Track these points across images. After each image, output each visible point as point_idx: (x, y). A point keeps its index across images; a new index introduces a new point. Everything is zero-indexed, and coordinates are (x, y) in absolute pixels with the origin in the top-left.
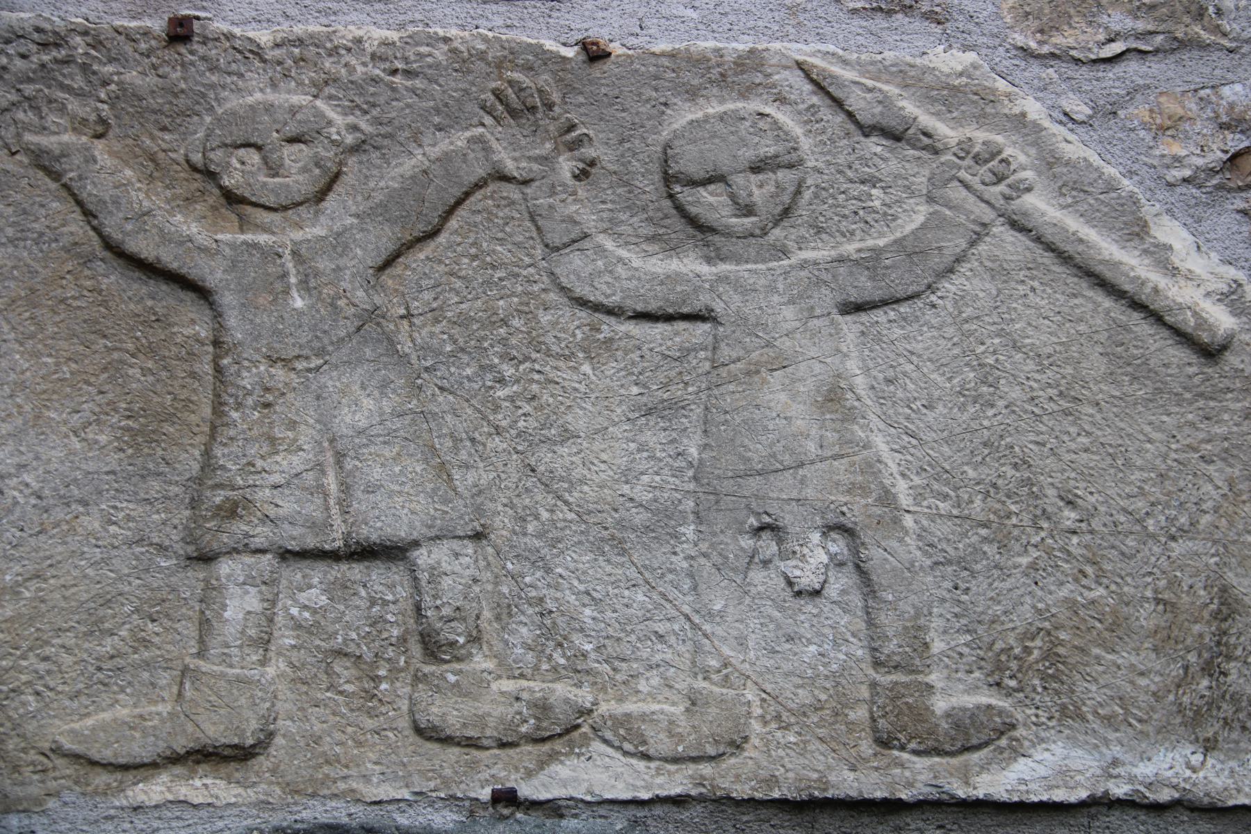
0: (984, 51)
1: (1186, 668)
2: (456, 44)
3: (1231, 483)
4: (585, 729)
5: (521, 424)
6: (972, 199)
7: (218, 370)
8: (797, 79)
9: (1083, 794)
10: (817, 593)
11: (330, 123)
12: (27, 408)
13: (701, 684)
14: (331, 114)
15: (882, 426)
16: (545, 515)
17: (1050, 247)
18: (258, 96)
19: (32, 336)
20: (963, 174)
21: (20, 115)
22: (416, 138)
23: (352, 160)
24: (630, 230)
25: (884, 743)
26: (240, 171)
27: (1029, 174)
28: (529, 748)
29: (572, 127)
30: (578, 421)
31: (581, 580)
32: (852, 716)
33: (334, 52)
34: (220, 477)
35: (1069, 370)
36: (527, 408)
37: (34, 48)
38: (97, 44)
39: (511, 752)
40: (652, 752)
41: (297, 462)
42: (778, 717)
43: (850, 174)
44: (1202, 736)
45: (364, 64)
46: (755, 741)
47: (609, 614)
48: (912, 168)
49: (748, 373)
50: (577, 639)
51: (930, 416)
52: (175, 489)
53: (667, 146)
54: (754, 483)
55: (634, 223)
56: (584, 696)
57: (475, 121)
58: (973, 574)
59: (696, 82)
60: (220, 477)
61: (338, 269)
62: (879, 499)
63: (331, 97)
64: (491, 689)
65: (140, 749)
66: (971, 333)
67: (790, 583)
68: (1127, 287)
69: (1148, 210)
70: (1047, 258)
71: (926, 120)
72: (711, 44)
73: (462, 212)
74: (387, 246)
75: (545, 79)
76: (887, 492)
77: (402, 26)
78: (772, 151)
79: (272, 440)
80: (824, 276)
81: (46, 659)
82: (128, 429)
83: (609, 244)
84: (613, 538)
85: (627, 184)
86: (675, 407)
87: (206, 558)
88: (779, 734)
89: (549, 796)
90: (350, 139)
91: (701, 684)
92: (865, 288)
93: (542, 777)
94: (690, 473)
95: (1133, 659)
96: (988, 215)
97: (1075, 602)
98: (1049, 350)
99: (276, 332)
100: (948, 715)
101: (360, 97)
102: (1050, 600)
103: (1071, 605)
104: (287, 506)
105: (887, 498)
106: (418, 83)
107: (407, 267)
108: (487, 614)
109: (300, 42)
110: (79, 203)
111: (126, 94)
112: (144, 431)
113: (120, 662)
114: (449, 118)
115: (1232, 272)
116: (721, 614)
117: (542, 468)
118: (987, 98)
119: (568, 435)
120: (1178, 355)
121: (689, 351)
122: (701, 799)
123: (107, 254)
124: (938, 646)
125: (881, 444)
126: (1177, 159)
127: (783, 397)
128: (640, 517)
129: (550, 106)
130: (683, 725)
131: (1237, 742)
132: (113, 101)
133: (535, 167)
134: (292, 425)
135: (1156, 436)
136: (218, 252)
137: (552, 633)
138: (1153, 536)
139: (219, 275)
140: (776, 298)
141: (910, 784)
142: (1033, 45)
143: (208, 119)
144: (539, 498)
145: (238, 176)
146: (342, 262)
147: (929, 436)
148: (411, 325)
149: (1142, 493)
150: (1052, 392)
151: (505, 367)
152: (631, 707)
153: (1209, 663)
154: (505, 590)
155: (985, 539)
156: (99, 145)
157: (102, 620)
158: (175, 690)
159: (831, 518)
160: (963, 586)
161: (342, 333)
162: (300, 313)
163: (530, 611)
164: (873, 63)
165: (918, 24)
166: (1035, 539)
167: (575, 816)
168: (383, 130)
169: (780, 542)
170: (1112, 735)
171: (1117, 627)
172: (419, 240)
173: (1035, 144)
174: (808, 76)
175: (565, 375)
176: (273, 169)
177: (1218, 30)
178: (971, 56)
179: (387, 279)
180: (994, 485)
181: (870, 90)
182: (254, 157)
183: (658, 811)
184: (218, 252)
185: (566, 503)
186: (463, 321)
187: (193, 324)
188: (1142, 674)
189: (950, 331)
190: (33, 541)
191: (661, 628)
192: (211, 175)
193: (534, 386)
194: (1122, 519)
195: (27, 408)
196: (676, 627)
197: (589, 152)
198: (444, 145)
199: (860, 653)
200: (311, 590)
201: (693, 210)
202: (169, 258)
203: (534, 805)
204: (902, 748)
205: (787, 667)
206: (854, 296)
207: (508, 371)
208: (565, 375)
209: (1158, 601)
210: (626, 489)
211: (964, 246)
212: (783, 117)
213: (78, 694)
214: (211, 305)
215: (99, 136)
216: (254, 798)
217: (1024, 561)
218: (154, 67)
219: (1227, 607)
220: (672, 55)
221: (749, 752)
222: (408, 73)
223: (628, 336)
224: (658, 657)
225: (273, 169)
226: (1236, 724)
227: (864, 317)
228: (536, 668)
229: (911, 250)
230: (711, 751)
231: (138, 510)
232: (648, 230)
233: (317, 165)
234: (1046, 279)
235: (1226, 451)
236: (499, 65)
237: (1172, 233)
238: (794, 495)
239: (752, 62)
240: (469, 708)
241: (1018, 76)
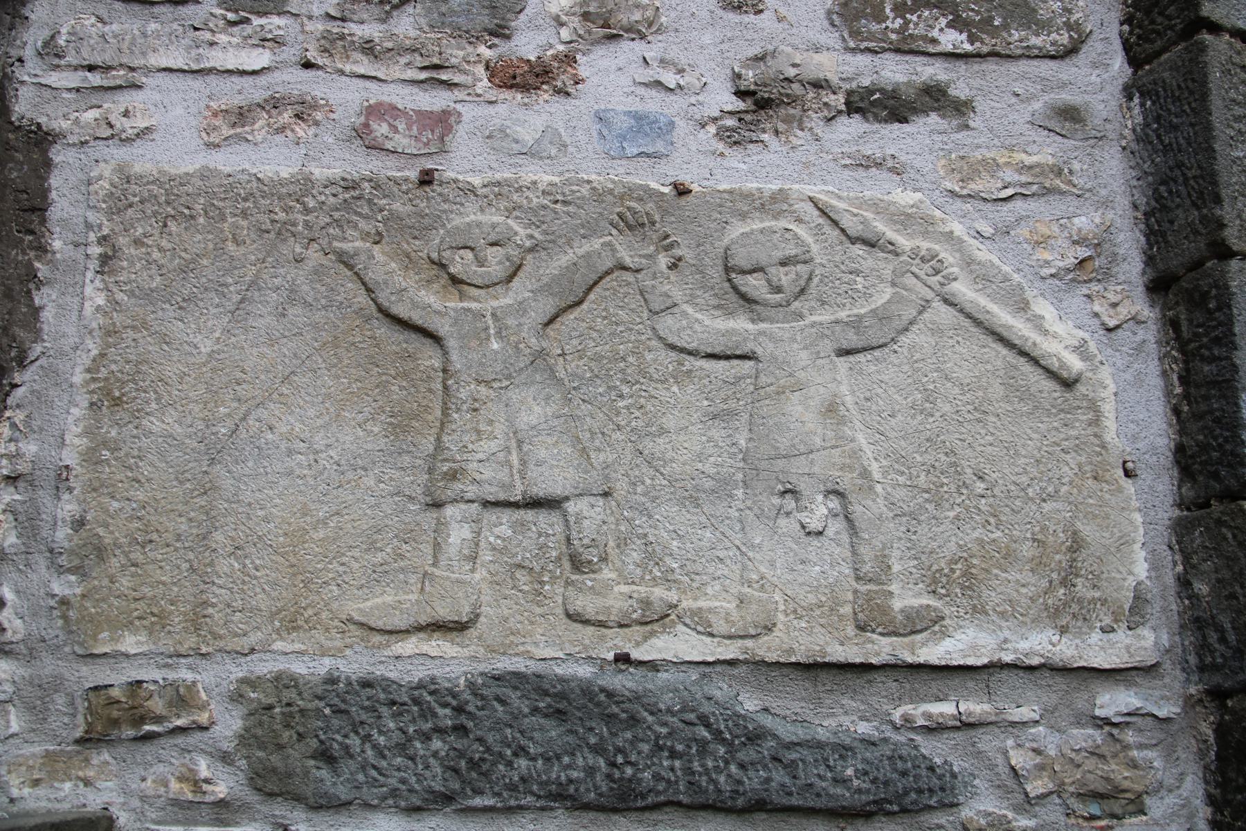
0: (926, 192)
1: (1051, 582)
2: (594, 185)
3: (1080, 466)
4: (673, 617)
5: (634, 424)
6: (920, 284)
7: (446, 387)
8: (809, 207)
9: (985, 661)
10: (820, 533)
11: (516, 234)
12: (332, 410)
13: (746, 590)
14: (517, 228)
15: (862, 427)
16: (648, 482)
17: (969, 316)
18: (472, 217)
19: (335, 366)
20: (914, 269)
21: (331, 231)
22: (569, 243)
23: (529, 257)
24: (703, 302)
25: (862, 628)
26: (461, 264)
27: (955, 270)
28: (638, 628)
29: (667, 237)
30: (670, 422)
31: (671, 523)
32: (842, 611)
33: (519, 190)
34: (447, 454)
35: (980, 394)
36: (637, 414)
37: (341, 190)
38: (377, 187)
39: (626, 630)
40: (715, 632)
41: (493, 446)
42: (795, 611)
43: (843, 267)
44: (1060, 623)
45: (538, 197)
46: (780, 626)
47: (689, 545)
48: (882, 264)
49: (778, 393)
50: (668, 560)
51: (893, 421)
52: (419, 462)
53: (727, 249)
54: (781, 463)
55: (705, 297)
56: (673, 596)
57: (606, 232)
58: (919, 522)
59: (745, 209)
60: (447, 454)
61: (520, 324)
62: (860, 474)
63: (517, 218)
64: (613, 591)
65: (400, 622)
66: (919, 369)
67: (803, 527)
68: (1016, 342)
69: (1029, 294)
70: (967, 323)
71: (891, 234)
72: (755, 185)
73: (597, 289)
74: (550, 310)
75: (650, 206)
76: (865, 469)
77: (561, 174)
78: (793, 252)
79: (478, 432)
80: (826, 332)
81: (343, 564)
82: (391, 424)
83: (690, 310)
84: (691, 497)
85: (702, 272)
86: (732, 414)
87: (437, 505)
88: (795, 622)
89: (650, 658)
90: (528, 244)
91: (746, 590)
92: (852, 340)
93: (646, 646)
94: (741, 456)
95: (1018, 576)
96: (930, 295)
97: (983, 540)
98: (968, 381)
99: (482, 364)
100: (902, 611)
101: (534, 217)
102: (967, 539)
103: (980, 542)
104: (488, 473)
105: (865, 474)
106: (571, 209)
107: (562, 324)
108: (611, 544)
109: (499, 184)
110: (364, 284)
111: (394, 217)
113: (386, 568)
114: (590, 230)
115: (1081, 334)
116: (760, 546)
117: (646, 452)
118: (929, 221)
119: (663, 431)
120: (1048, 385)
121: (740, 378)
122: (746, 662)
123: (380, 315)
124: (896, 568)
125: (861, 439)
126: (1047, 262)
127: (800, 408)
128: (708, 484)
129: (653, 223)
130: (735, 615)
131: (1080, 628)
132: (385, 221)
133: (644, 261)
134: (490, 423)
135: (1035, 436)
136: (446, 314)
137: (652, 556)
138: (1032, 499)
139: (447, 328)
140: (795, 346)
141: (878, 654)
142: (957, 189)
143: (442, 232)
144: (644, 470)
145: (459, 266)
146: (522, 320)
147: (893, 434)
148: (565, 360)
149: (1026, 472)
150: (970, 407)
151: (623, 387)
152: (701, 603)
153: (1065, 579)
154: (623, 528)
155: (927, 500)
156: (377, 248)
157: (375, 542)
158: (419, 586)
159: (830, 486)
160: (913, 530)
161: (522, 365)
162: (497, 352)
163: (639, 542)
164: (857, 198)
165: (886, 175)
166: (959, 501)
167: (667, 671)
168: (549, 238)
169: (797, 500)
170: (1004, 624)
171: (1009, 556)
172: (570, 307)
173: (959, 250)
174: (816, 206)
175: (662, 393)
176: (481, 262)
177: (1070, 183)
178: (919, 195)
179: (550, 331)
180: (933, 466)
181: (856, 215)
182: (469, 255)
183: (718, 668)
184: (446, 314)
185: (662, 474)
186: (598, 358)
187: (430, 358)
188: (1023, 586)
189: (906, 368)
190: (335, 492)
191: (721, 554)
192: (443, 266)
193: (642, 400)
194: (1013, 488)
195: (332, 410)
196: (731, 554)
197: (678, 252)
198: (586, 247)
199: (847, 571)
200: (502, 525)
201: (743, 289)
202: (417, 317)
203: (641, 663)
204: (873, 631)
205: (801, 580)
206: (845, 345)
207: (625, 390)
208: (662, 393)
209: (1034, 540)
210: (700, 466)
211: (915, 314)
212: (800, 231)
213: (362, 587)
214: (442, 346)
215: (376, 243)
216: (467, 654)
217: (951, 514)
218: (410, 200)
219: (1076, 544)
220: (731, 192)
221: (776, 633)
222: (565, 203)
223: (701, 369)
224: (719, 573)
225: (481, 262)
226: (1080, 617)
227: (851, 358)
228: (642, 578)
229: (881, 316)
230: (752, 632)
231: (397, 474)
232: (714, 302)
233: (508, 259)
234: (966, 336)
235: (1077, 446)
236: (622, 198)
237: (1044, 308)
238: (807, 471)
239: (780, 197)
240: (600, 602)
241: (948, 208)
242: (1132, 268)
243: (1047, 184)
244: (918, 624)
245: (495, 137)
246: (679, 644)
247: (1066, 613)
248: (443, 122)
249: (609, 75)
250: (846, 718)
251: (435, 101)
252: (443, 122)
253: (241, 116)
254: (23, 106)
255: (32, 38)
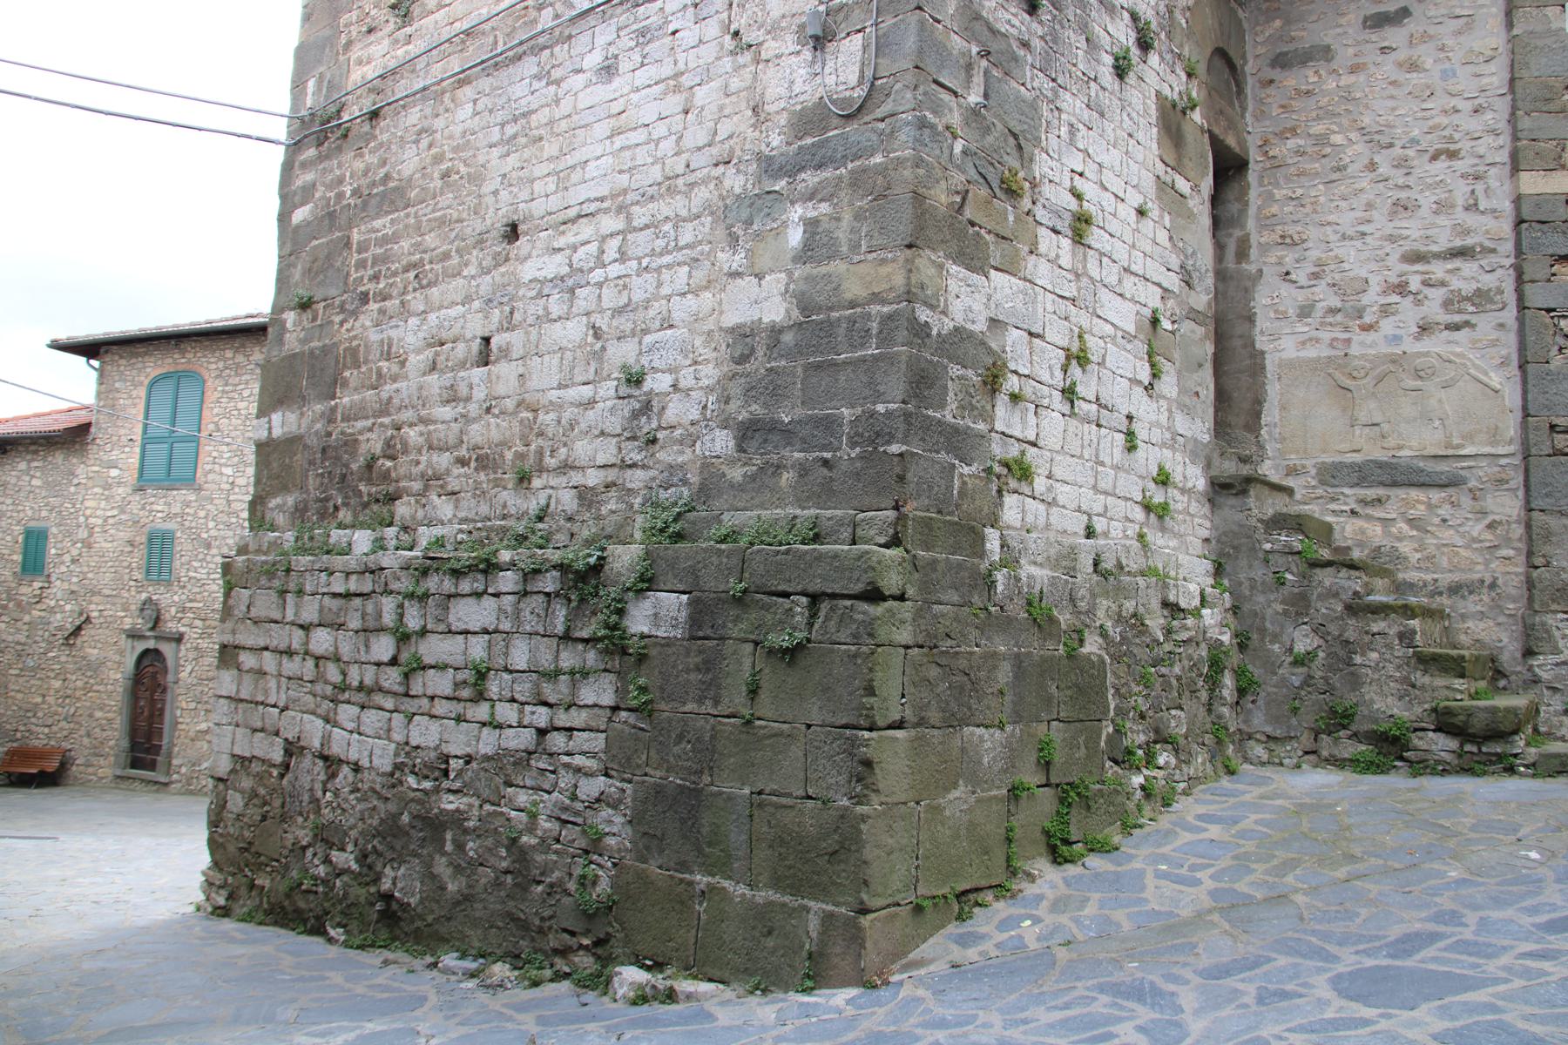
26: (1355, 374)
101: (1370, 361)
112: (1344, 410)
137: (1400, 434)
200: (1367, 430)
237: (1492, 374)
242: (1515, 363)
243: (1494, 343)
244: (1459, 447)
245: (1362, 344)
246: (1406, 453)
247: (1493, 444)
248: (1348, 341)
249: (1387, 326)
250: (1443, 467)
251: (1346, 336)
252: (1348, 341)
253: (1303, 343)
254: (1258, 346)
255: (1258, 330)
